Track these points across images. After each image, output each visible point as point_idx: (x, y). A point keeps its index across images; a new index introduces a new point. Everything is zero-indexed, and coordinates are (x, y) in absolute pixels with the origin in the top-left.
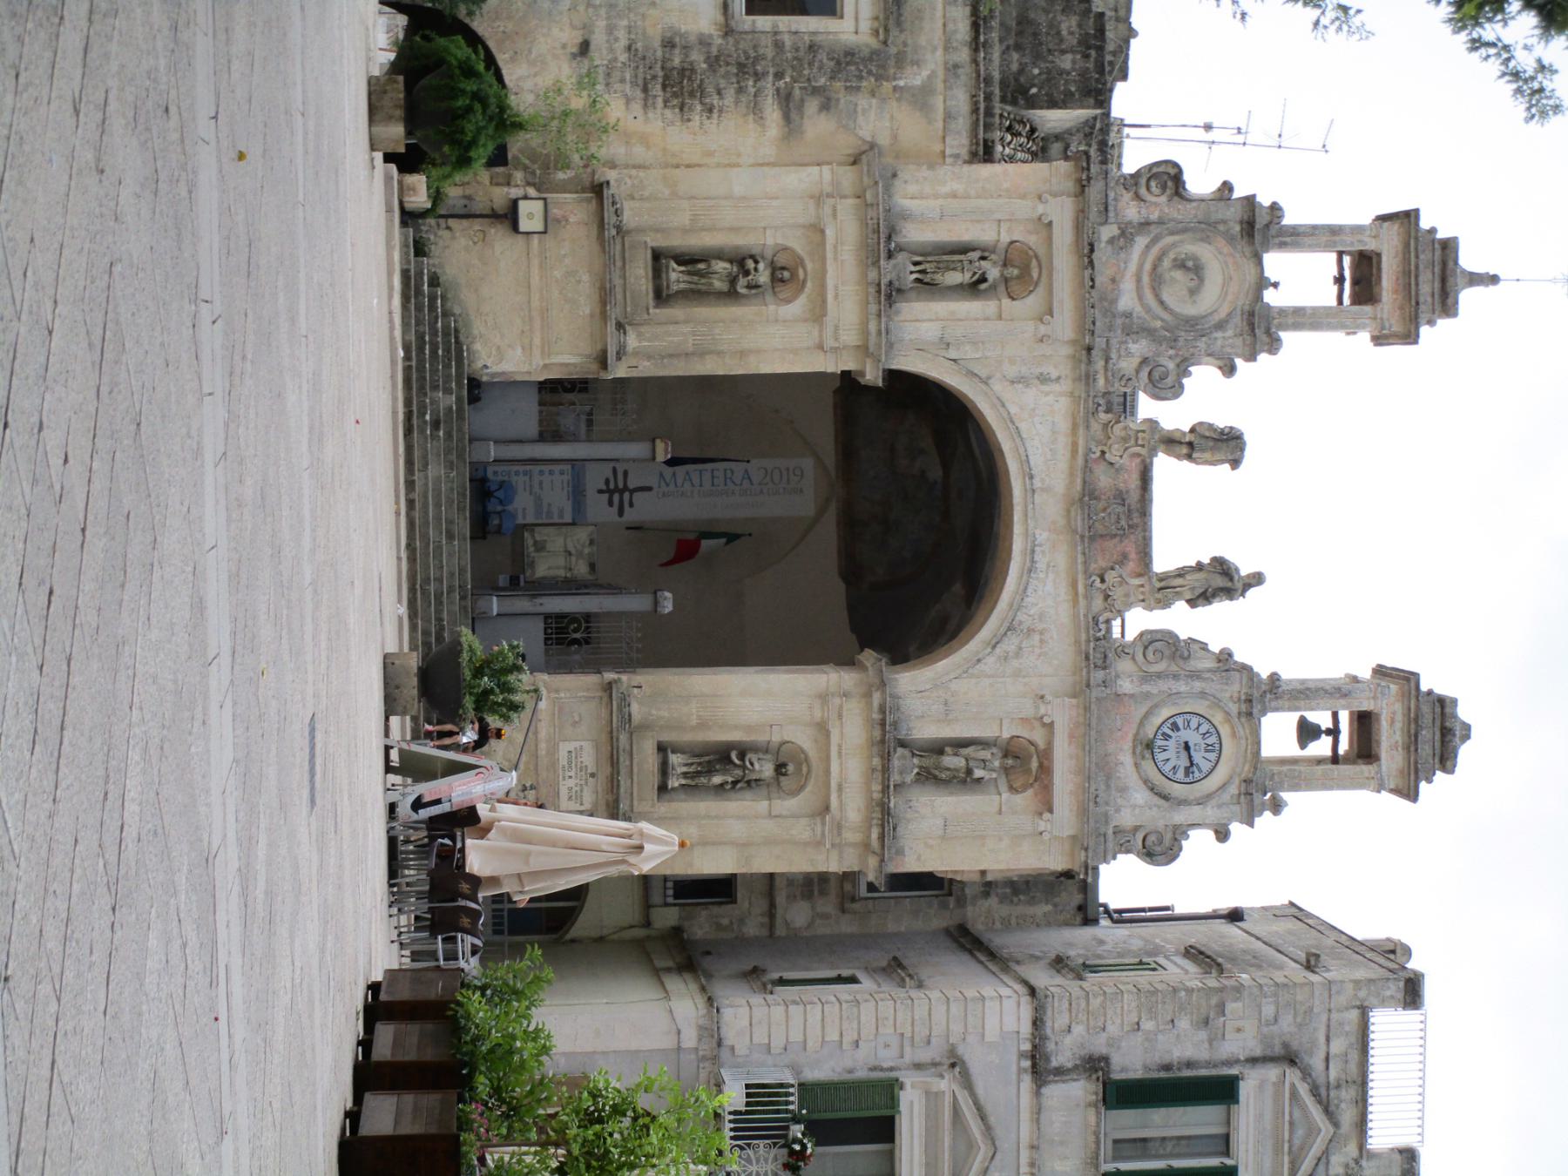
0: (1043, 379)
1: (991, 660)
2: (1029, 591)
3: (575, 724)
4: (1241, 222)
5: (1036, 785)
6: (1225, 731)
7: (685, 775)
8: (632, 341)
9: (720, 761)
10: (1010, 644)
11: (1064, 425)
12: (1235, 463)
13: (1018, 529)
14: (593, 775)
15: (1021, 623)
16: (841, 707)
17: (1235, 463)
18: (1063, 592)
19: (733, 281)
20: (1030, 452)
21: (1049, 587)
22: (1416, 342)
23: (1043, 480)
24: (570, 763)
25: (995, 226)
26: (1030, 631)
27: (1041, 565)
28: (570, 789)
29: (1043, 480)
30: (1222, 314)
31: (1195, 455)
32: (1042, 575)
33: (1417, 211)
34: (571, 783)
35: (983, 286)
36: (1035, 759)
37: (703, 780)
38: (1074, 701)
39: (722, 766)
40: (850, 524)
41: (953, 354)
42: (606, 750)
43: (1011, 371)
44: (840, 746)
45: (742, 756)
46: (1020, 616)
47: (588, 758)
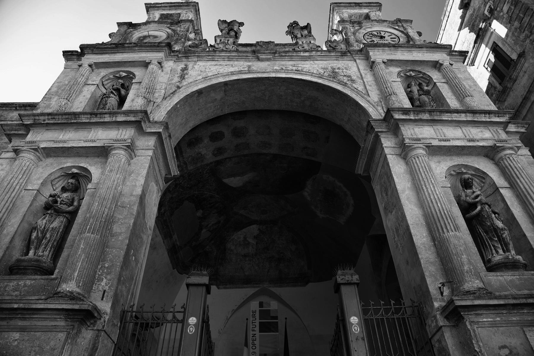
0: (185, 69)
4: (129, 28)
5: (424, 72)
6: (369, 30)
7: (506, 250)
8: (70, 287)
9: (482, 224)
11: (214, 63)
12: (242, 24)
13: (273, 75)
16: (409, 139)
17: (242, 24)
19: (59, 212)
20: (225, 71)
21: (307, 66)
22: (198, 3)
23: (244, 68)
25: (89, 86)
26: (333, 72)
27: (294, 68)
29: (244, 68)
30: (169, 31)
31: (235, 30)
33: (146, 4)
35: (123, 92)
36: (408, 74)
37: (506, 234)
38: (371, 53)
40: (281, 280)
41: (159, 100)
43: (176, 79)
44: (440, 140)
45: (473, 206)
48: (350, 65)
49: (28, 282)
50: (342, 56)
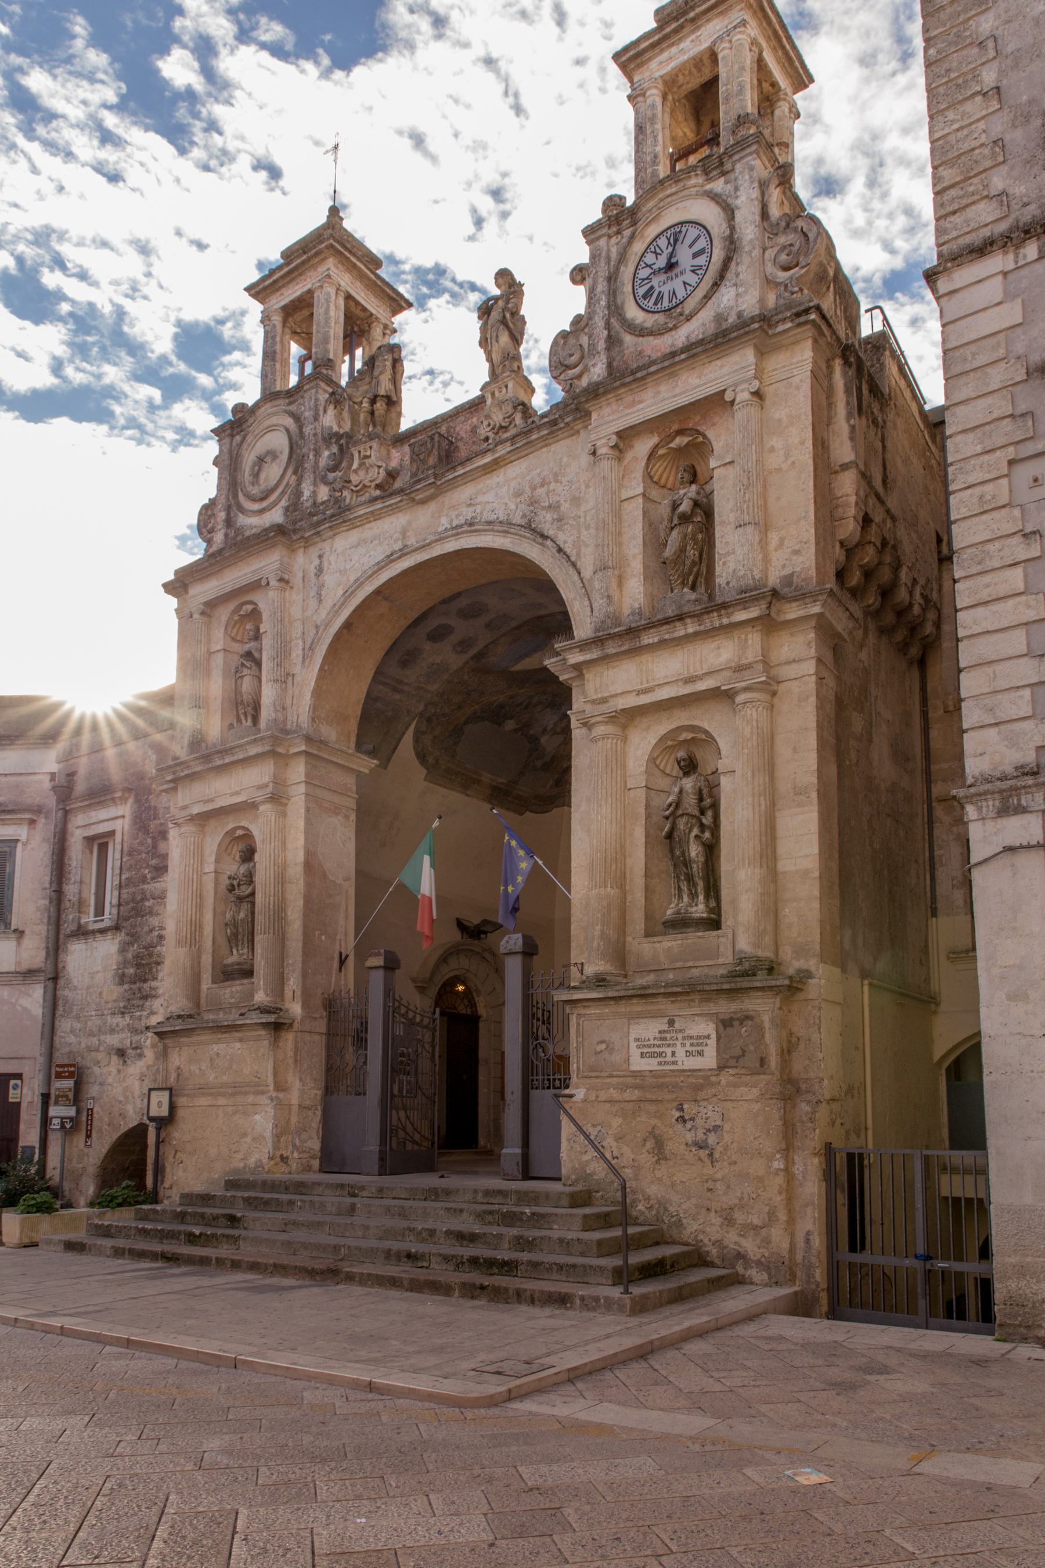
1: (561, 538)
2: (493, 517)
3: (610, 1048)
10: (546, 521)
14: (671, 1023)
15: (524, 516)
18: (498, 478)
24: (652, 1055)
26: (533, 502)
28: (688, 1053)
32: (479, 509)
34: (680, 1052)
39: (688, 838)
42: (637, 1006)
46: (517, 519)
47: (649, 1029)
48: (565, 460)
49: (239, 988)
50: (552, 433)
